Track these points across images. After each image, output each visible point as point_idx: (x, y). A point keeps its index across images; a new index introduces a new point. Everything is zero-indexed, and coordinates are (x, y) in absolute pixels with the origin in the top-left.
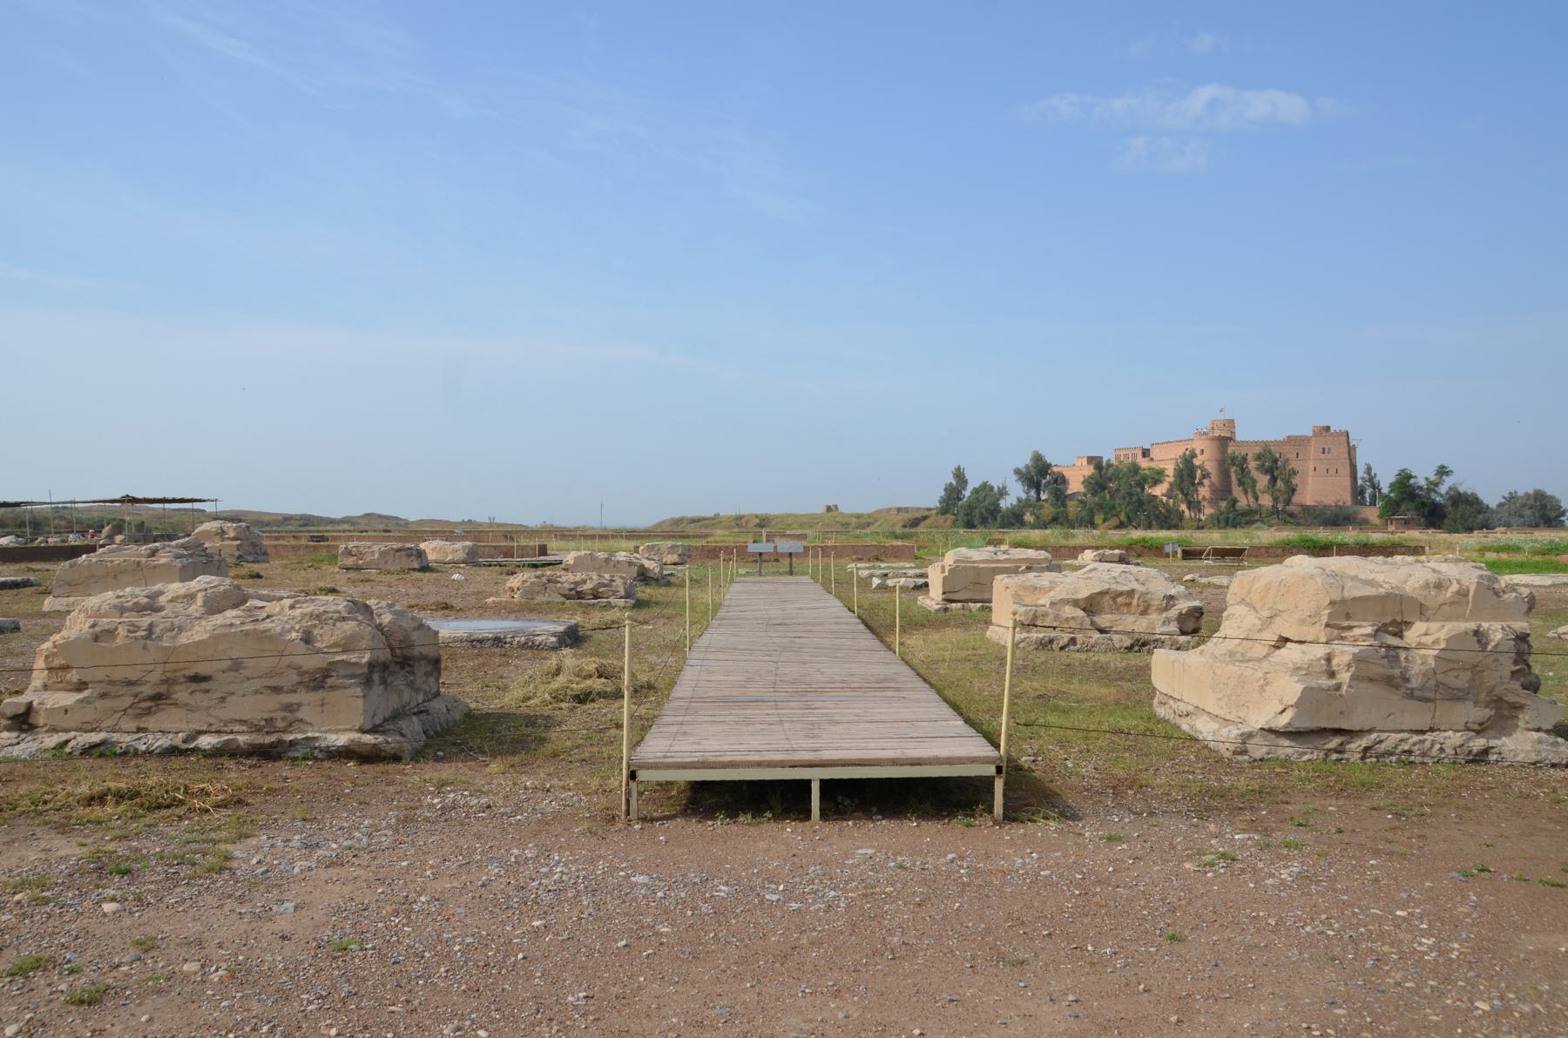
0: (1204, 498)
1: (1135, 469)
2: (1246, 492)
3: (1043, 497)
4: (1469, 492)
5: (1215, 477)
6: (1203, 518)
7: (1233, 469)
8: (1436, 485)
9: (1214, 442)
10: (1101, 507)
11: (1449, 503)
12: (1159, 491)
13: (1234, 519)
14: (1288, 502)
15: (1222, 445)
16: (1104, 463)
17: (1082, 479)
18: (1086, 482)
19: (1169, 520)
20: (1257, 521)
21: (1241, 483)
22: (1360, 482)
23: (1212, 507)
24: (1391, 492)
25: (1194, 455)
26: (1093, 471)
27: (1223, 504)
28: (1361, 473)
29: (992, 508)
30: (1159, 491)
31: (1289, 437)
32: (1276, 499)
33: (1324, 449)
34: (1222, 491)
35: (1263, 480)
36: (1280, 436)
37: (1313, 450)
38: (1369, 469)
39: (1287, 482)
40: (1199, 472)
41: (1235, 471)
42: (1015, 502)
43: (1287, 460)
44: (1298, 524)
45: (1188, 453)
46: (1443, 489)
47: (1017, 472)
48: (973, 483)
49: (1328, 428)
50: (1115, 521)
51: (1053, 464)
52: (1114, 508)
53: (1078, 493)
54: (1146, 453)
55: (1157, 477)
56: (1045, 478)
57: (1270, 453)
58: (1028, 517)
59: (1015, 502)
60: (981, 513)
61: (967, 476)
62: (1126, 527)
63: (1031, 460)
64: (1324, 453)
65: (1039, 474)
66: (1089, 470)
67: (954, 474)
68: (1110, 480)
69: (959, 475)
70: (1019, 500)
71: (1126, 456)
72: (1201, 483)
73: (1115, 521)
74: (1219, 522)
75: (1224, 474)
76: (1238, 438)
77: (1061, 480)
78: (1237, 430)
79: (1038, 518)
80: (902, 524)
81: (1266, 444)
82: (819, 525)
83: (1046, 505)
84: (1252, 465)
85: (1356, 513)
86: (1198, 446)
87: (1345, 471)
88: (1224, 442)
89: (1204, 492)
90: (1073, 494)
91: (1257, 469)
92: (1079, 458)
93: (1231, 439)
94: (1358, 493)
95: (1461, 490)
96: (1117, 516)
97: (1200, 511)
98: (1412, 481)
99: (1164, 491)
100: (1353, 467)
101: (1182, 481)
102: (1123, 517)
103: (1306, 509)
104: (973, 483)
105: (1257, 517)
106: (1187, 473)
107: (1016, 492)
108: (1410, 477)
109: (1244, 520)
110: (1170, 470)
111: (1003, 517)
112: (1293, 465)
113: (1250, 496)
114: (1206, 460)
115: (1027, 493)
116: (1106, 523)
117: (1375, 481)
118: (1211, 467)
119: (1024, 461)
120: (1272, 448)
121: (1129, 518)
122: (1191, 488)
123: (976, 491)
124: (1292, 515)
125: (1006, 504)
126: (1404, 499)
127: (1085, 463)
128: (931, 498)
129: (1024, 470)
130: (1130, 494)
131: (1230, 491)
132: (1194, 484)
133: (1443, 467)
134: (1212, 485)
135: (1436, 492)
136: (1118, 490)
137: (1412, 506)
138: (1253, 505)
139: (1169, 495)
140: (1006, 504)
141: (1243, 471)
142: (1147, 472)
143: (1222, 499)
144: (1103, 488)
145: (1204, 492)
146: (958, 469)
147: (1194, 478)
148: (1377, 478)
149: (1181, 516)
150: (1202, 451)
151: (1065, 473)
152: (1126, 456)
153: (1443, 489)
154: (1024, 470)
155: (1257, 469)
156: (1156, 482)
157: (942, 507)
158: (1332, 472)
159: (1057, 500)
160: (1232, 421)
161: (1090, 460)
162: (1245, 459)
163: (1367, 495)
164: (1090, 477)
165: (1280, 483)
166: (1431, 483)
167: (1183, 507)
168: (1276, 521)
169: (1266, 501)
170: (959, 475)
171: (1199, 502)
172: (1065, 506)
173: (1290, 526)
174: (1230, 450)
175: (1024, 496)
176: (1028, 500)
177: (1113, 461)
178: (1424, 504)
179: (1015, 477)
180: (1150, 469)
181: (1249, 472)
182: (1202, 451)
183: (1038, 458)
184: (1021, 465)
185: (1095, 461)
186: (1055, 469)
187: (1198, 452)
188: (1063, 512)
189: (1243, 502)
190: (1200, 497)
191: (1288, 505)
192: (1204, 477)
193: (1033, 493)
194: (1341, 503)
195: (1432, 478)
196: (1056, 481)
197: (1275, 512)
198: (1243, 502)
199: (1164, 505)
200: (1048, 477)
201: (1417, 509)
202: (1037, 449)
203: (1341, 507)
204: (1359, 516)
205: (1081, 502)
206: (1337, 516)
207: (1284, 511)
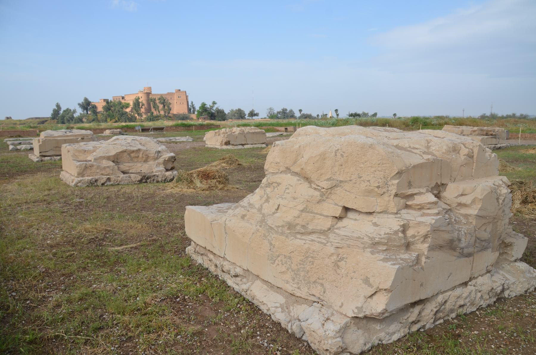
0: (143, 112)
1: (120, 103)
2: (156, 110)
3: (89, 113)
4: (222, 109)
5: (146, 105)
6: (143, 119)
7: (151, 103)
8: (212, 107)
10: (109, 116)
11: (216, 113)
12: (128, 110)
13: (153, 119)
14: (169, 113)
16: (109, 101)
17: (102, 107)
18: (104, 107)
19: (132, 119)
20: (160, 119)
21: (154, 107)
22: (190, 107)
23: (145, 115)
24: (200, 109)
25: (139, 98)
26: (106, 104)
27: (149, 114)
28: (190, 104)
29: (71, 116)
30: (128, 110)
31: (168, 93)
32: (165, 112)
33: (179, 97)
34: (148, 110)
35: (161, 106)
36: (165, 92)
37: (176, 97)
38: (192, 103)
39: (168, 107)
40: (141, 104)
41: (152, 104)
42: (79, 115)
43: (168, 100)
44: (172, 120)
45: (137, 98)
46: (214, 108)
47: (79, 104)
48: (63, 108)
49: (180, 90)
50: (114, 120)
51: (92, 102)
52: (114, 116)
53: (101, 111)
54: (123, 98)
55: (127, 105)
56: (89, 106)
57: (163, 98)
58: (84, 120)
59: (79, 115)
60: (67, 119)
61: (61, 106)
62: (118, 122)
63: (84, 100)
64: (179, 97)
65: (87, 105)
66: (104, 104)
68: (112, 107)
69: (58, 106)
70: (81, 114)
71: (117, 99)
72: (142, 107)
73: (114, 120)
74: (148, 120)
75: (149, 104)
76: (153, 93)
77: (95, 107)
78: (152, 90)
79: (88, 120)
80: (37, 123)
81: (161, 95)
83: (90, 115)
84: (157, 101)
85: (189, 116)
86: (140, 95)
87: (186, 103)
88: (148, 94)
89: (143, 110)
90: (99, 112)
91: (159, 103)
92: (100, 100)
93: (150, 93)
94: (189, 110)
95: (219, 108)
96: (114, 118)
97: (142, 116)
98: (206, 106)
99: (130, 110)
100: (188, 102)
101: (136, 107)
102: (117, 119)
103: (174, 115)
104: (63, 108)
105: (160, 118)
106: (137, 104)
107: (79, 111)
108: (205, 105)
109: (156, 119)
110: (131, 103)
111: (75, 120)
112: (170, 101)
113: (157, 111)
114: (143, 100)
115: (83, 112)
116: (111, 121)
117: (194, 107)
118: (144, 102)
119: (81, 101)
120: (163, 96)
121: (119, 119)
122: (139, 109)
123: (64, 111)
124: (170, 117)
125: (76, 115)
126: (203, 112)
127: (103, 101)
128: (48, 113)
129: (81, 104)
130: (119, 111)
131: (151, 111)
132: (139, 108)
133: (214, 102)
134: (145, 108)
135: (212, 109)
136: (115, 110)
137: (206, 113)
138: (158, 114)
139: (132, 111)
140: (76, 115)
141: (155, 104)
142: (124, 104)
143: (149, 113)
144: (110, 109)
145: (143, 110)
146: (58, 104)
147: (139, 106)
148: (195, 106)
149: (136, 118)
150: (141, 97)
151: (96, 105)
152: (117, 99)
153: (214, 108)
154: (81, 104)
155: (159, 103)
156: (127, 107)
157: (53, 117)
158: (181, 104)
159: (94, 114)
160: (150, 88)
161: (105, 100)
162: (155, 100)
163: (192, 111)
164: (105, 106)
165: (166, 107)
166: (211, 106)
167: (136, 115)
168: (165, 119)
169: (162, 113)
170: (58, 106)
171: (141, 114)
172: (97, 115)
173: (170, 121)
174: (150, 97)
175: (82, 113)
176: (84, 114)
177: (112, 100)
178: (209, 113)
179: (78, 106)
180: (125, 103)
181: (156, 104)
182: (141, 97)
183: (86, 100)
184: (80, 102)
185: (106, 101)
186: (93, 103)
187: (140, 97)
188: (96, 118)
189: (155, 113)
190: (142, 112)
191: (169, 114)
192: (142, 105)
193: (85, 112)
194: (185, 113)
195: (211, 105)
196: (93, 107)
197: (165, 116)
198: (155, 113)
199: (130, 115)
200: (90, 106)
201: (207, 114)
203: (185, 114)
204: (190, 117)
205: (102, 114)
206: (184, 117)
207: (168, 116)
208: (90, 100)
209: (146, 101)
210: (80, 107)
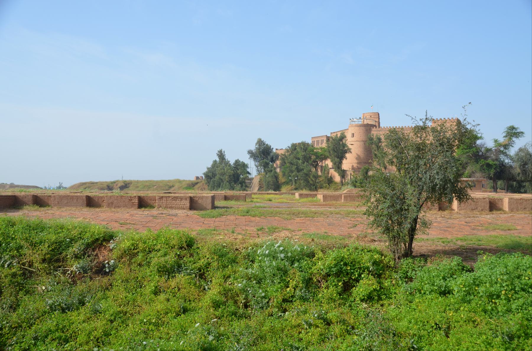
9: (362, 128)
15: (367, 130)
47: (250, 152)
67: (218, 155)
69: (221, 155)
82: (156, 187)
88: (368, 128)
142: (320, 151)
146: (220, 152)
170: (221, 155)
179: (248, 156)
183: (260, 142)
202: (261, 138)
208: (268, 141)
209: (362, 143)
210: (251, 157)
